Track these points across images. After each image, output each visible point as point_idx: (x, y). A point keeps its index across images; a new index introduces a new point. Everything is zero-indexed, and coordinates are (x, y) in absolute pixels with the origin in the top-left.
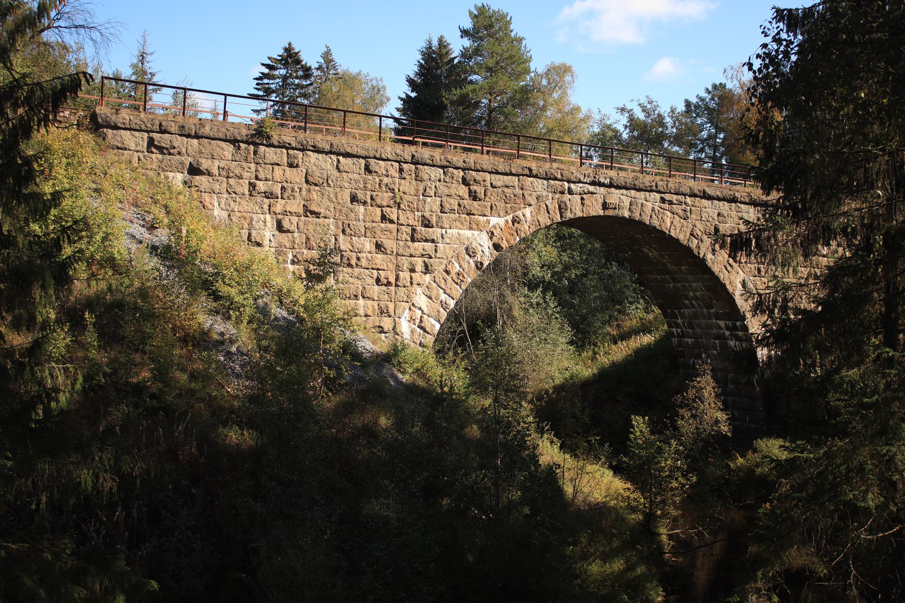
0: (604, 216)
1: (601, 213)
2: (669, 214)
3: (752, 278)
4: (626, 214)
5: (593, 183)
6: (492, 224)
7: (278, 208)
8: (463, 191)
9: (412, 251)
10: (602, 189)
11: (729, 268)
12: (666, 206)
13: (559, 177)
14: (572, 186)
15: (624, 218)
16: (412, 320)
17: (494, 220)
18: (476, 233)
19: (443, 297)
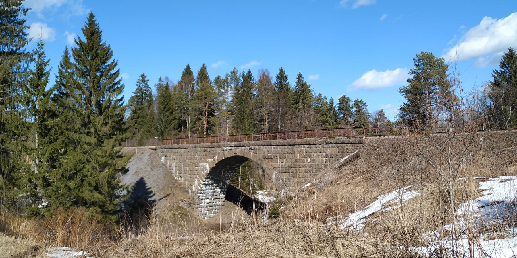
0: (235, 156)
1: (234, 155)
2: (251, 153)
3: (279, 173)
4: (240, 155)
5: (230, 147)
6: (209, 161)
7: (176, 162)
8: (204, 153)
9: (194, 170)
10: (233, 148)
11: (270, 170)
12: (251, 150)
13: (222, 146)
14: (226, 148)
15: (239, 156)
16: (195, 186)
17: (210, 160)
18: (206, 164)
19: (201, 181)
